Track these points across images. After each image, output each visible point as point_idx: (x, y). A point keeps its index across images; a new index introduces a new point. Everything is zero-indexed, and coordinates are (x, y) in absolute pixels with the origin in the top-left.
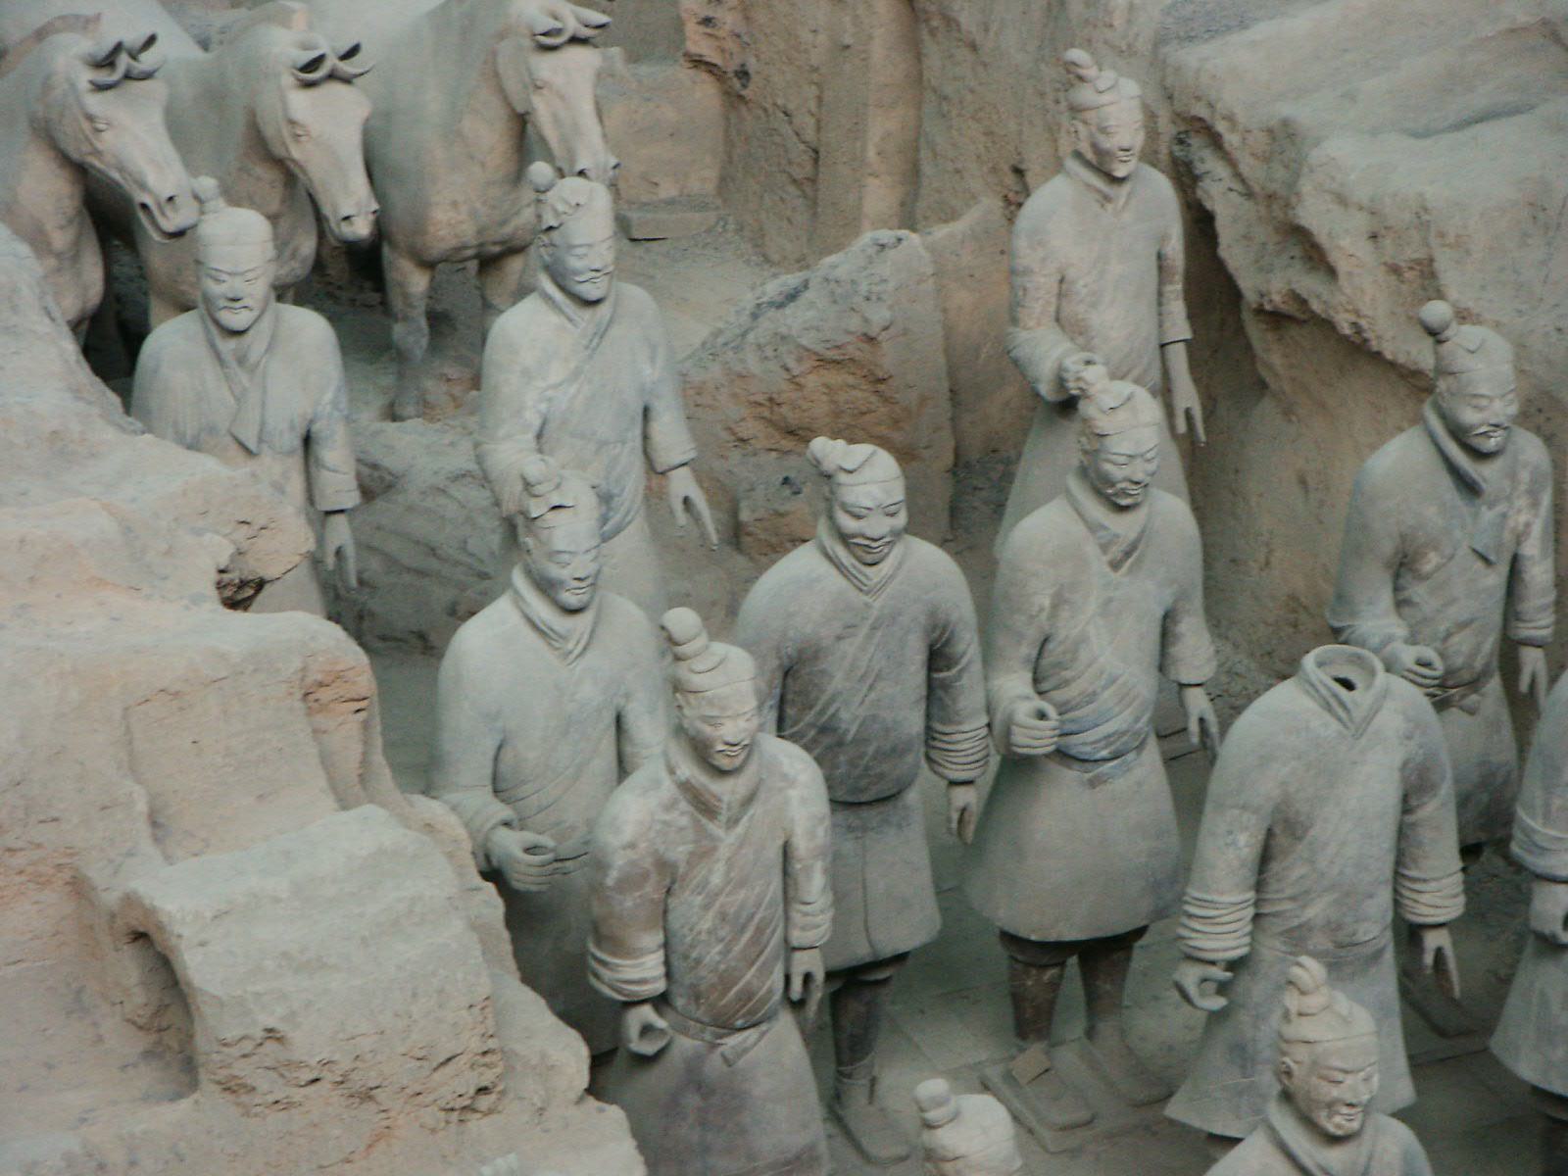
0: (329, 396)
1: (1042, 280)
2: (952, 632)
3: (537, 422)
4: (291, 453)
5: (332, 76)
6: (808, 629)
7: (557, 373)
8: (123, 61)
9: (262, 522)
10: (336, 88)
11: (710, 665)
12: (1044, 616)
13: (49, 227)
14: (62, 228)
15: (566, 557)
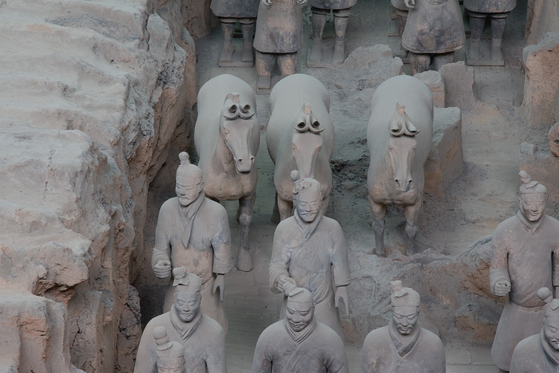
0: (218, 234)
1: (499, 251)
2: (331, 363)
3: (286, 259)
4: (203, 250)
5: (309, 130)
6: (275, 349)
7: (294, 244)
8: (238, 111)
9: (66, 266)
10: (308, 134)
11: (162, 349)
12: (374, 366)
13: (223, 162)
14: (226, 163)
15: (181, 302)
